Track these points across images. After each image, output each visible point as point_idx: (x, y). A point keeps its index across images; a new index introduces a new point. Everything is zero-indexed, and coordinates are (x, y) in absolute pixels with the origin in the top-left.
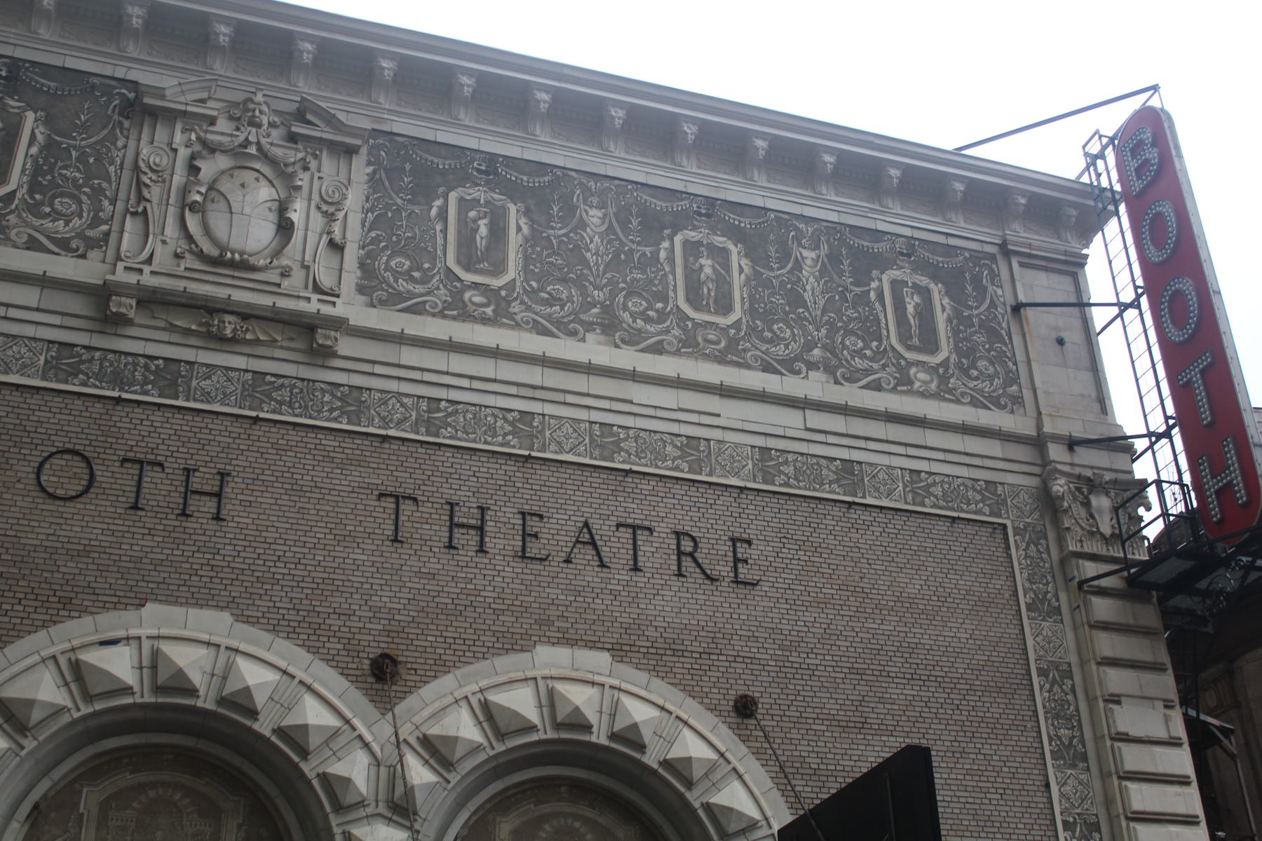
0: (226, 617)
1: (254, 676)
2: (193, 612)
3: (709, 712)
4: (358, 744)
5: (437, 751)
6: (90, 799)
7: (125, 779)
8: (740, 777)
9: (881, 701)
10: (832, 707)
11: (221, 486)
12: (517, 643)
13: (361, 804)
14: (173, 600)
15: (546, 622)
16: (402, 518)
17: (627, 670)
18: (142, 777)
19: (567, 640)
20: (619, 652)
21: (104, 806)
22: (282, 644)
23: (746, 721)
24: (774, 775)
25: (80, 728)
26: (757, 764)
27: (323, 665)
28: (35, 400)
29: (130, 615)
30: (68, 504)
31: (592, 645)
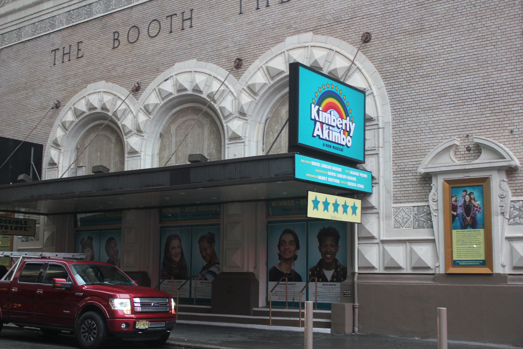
0: (195, 60)
1: (200, 80)
2: (186, 62)
3: (351, 45)
4: (230, 94)
5: (251, 90)
6: (173, 128)
7: (181, 120)
8: (360, 70)
9: (432, 15)
10: (407, 26)
11: (191, 15)
12: (279, 39)
13: (231, 114)
14: (182, 60)
15: (289, 27)
16: (242, 3)
17: (319, 37)
18: (184, 119)
19: (298, 32)
20: (315, 30)
21: (176, 130)
22: (210, 65)
23: (366, 44)
24: (377, 65)
25: (164, 108)
26: (370, 63)
27: (221, 69)
28: (145, 6)
29: (171, 69)
30: (156, 38)
31: (306, 31)
